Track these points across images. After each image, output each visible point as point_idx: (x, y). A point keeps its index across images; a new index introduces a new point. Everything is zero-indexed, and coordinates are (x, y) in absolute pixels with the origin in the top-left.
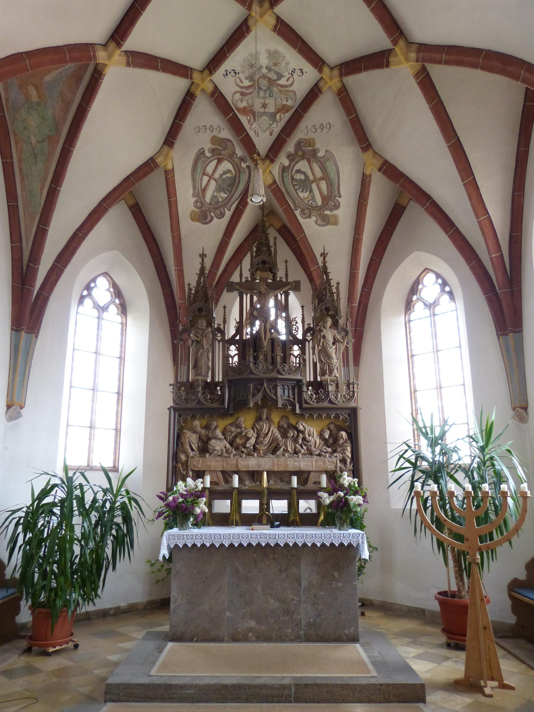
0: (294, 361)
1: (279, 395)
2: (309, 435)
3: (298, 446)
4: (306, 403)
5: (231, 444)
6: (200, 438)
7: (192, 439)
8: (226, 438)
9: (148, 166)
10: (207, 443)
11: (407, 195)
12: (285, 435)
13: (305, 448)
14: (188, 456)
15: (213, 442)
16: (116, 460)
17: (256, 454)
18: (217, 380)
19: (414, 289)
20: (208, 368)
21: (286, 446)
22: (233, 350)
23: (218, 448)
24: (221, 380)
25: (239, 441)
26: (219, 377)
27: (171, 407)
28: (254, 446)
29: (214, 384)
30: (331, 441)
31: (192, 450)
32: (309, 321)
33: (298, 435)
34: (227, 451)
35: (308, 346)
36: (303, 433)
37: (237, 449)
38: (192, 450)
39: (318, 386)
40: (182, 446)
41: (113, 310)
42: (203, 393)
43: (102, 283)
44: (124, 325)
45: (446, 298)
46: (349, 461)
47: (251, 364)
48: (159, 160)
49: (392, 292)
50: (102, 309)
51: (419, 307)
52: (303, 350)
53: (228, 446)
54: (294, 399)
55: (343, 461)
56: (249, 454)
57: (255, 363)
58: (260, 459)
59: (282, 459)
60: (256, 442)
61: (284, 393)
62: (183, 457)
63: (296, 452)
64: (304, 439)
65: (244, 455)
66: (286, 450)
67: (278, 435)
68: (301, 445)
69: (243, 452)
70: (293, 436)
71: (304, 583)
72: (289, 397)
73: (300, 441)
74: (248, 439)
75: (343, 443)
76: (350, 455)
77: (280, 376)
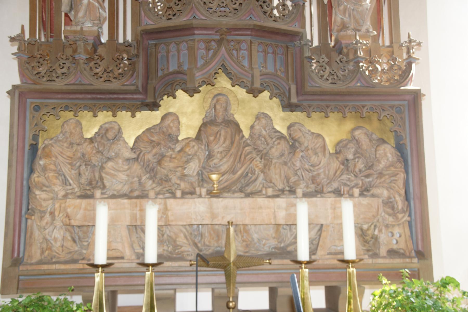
1: (255, 66)
5: (152, 172)
10: (102, 168)
17: (204, 191)
18: (121, 40)
25: (168, 164)
27: (15, 87)
28: (201, 174)
30: (360, 165)
31: (65, 182)
38: (65, 182)
42: (90, 59)
55: (389, 203)
58: (214, 200)
59: (261, 201)
61: (265, 61)
65: (179, 194)
70: (282, 155)
75: (387, 168)
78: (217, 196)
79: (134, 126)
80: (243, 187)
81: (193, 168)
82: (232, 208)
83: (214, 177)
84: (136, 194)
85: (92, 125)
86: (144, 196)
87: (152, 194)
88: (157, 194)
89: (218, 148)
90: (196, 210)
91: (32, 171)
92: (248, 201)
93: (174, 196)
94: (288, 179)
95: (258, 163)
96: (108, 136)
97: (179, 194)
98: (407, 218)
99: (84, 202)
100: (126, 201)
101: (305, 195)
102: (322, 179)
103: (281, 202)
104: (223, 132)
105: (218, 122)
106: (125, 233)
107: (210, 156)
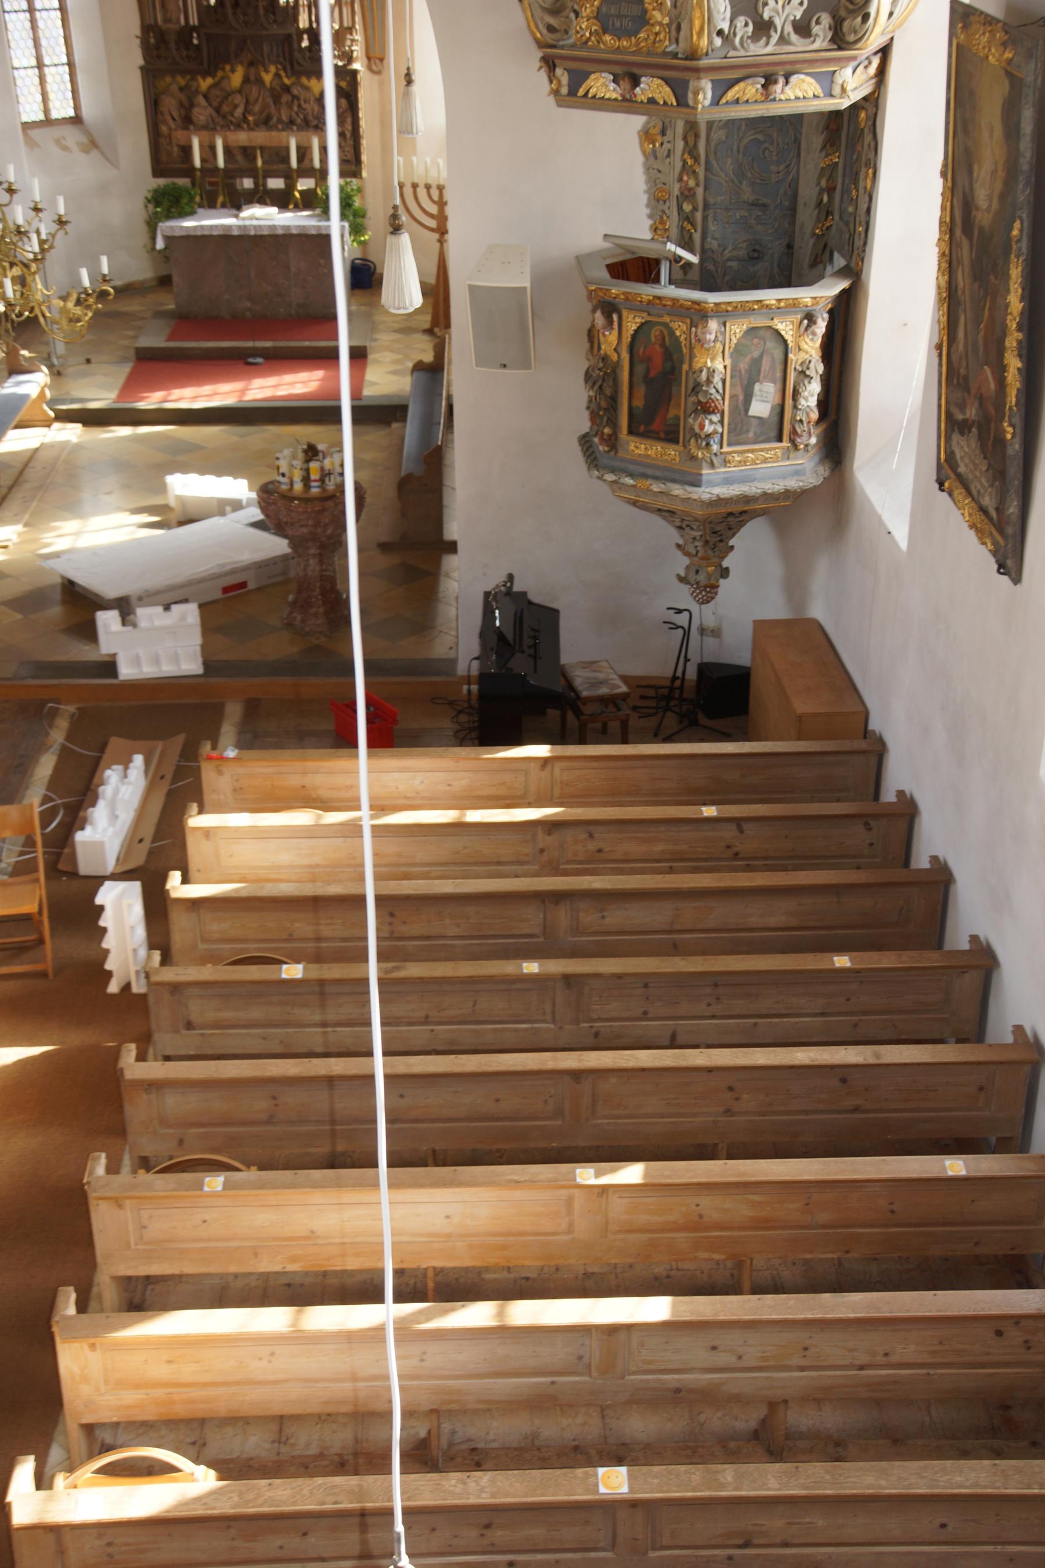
1: (266, 55)
2: (305, 102)
3: (293, 114)
4: (298, 63)
5: (218, 111)
6: (181, 105)
7: (170, 104)
8: (210, 105)
12: (277, 100)
13: (301, 116)
14: (170, 129)
15: (196, 111)
16: (77, 107)
18: (191, 23)
20: (179, 9)
21: (279, 113)
23: (202, 118)
24: (196, 23)
25: (225, 108)
26: (194, 20)
29: (189, 29)
31: (174, 119)
33: (292, 101)
34: (213, 121)
36: (298, 99)
37: (224, 117)
40: (162, 114)
46: (348, 134)
47: (230, 17)
53: (214, 114)
54: (284, 58)
56: (238, 127)
57: (234, 14)
59: (274, 133)
60: (245, 109)
62: (164, 129)
63: (292, 122)
64: (299, 106)
66: (280, 120)
67: (270, 100)
68: (297, 114)
69: (231, 122)
71: (293, 269)
72: (278, 56)
73: (296, 109)
74: (236, 106)
76: (350, 128)
77: (264, 33)
78: (252, 130)
79: (205, 83)
80: (266, 122)
81: (239, 111)
82: (259, 137)
83: (251, 118)
84: (211, 126)
85: (182, 81)
86: (214, 129)
87: (218, 128)
88: (222, 127)
89: (252, 99)
90: (242, 137)
91: (156, 113)
92: (268, 134)
93: (230, 129)
94: (291, 116)
95: (273, 109)
97: (232, 128)
98: (352, 142)
99: (185, 133)
100: (205, 133)
101: (300, 129)
102: (310, 118)
103: (284, 134)
104: (254, 89)
106: (208, 149)
107: (247, 103)
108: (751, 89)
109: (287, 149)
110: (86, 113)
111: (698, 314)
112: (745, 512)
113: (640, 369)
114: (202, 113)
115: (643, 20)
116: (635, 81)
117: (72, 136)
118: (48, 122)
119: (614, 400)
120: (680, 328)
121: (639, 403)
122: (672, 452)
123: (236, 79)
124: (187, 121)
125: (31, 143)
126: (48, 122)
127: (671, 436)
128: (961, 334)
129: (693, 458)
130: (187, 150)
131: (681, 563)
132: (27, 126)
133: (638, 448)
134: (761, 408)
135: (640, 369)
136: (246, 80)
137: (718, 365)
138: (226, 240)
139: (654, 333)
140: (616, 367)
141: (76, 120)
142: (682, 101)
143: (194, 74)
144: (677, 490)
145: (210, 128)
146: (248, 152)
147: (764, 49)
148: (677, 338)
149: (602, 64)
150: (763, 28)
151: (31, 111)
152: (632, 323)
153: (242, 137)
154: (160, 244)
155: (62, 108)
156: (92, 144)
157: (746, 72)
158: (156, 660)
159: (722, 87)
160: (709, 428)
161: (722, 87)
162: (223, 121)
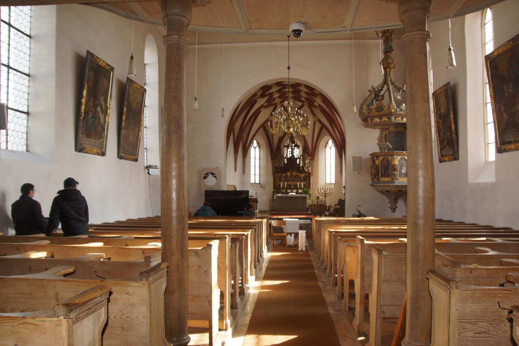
0: (298, 163)
9: (267, 121)
11: (323, 126)
19: (327, 143)
22: (285, 160)
26: (283, 165)
29: (282, 167)
32: (301, 154)
35: (301, 159)
39: (303, 167)
41: (257, 147)
43: (255, 142)
44: (260, 151)
45: (333, 146)
48: (270, 119)
49: (322, 143)
50: (255, 148)
51: (328, 147)
52: (300, 160)
79: (283, 175)
80: (294, 181)
85: (280, 174)
90: (289, 183)
96: (281, 176)
105: (291, 174)
108: (400, 118)
109: (297, 185)
110: (261, 182)
111: (392, 155)
112: (401, 191)
113: (383, 166)
114: (283, 179)
115: (383, 109)
116: (382, 118)
117: (259, 186)
118: (255, 183)
119: (378, 172)
120: (390, 158)
121: (383, 172)
122: (389, 179)
123: (289, 174)
124: (280, 181)
125: (252, 186)
126: (255, 183)
127: (389, 176)
128: (441, 134)
129: (393, 179)
130: (280, 185)
131: (389, 205)
132: (252, 183)
133: (383, 179)
134: (403, 171)
135: (383, 166)
136: (291, 174)
137: (397, 163)
138: (287, 197)
139: (385, 160)
140: (378, 166)
141: (260, 183)
142: (389, 119)
143: (282, 173)
144: (391, 184)
145: (284, 182)
146: (290, 185)
147: (402, 113)
148: (389, 160)
149: (376, 116)
150: (401, 110)
151: (252, 181)
152: (381, 159)
153: (289, 183)
154: (275, 198)
155: (257, 181)
156: (262, 187)
157: (399, 115)
158: (291, 229)
159: (395, 118)
160: (396, 173)
161: (395, 118)
162: (286, 179)
